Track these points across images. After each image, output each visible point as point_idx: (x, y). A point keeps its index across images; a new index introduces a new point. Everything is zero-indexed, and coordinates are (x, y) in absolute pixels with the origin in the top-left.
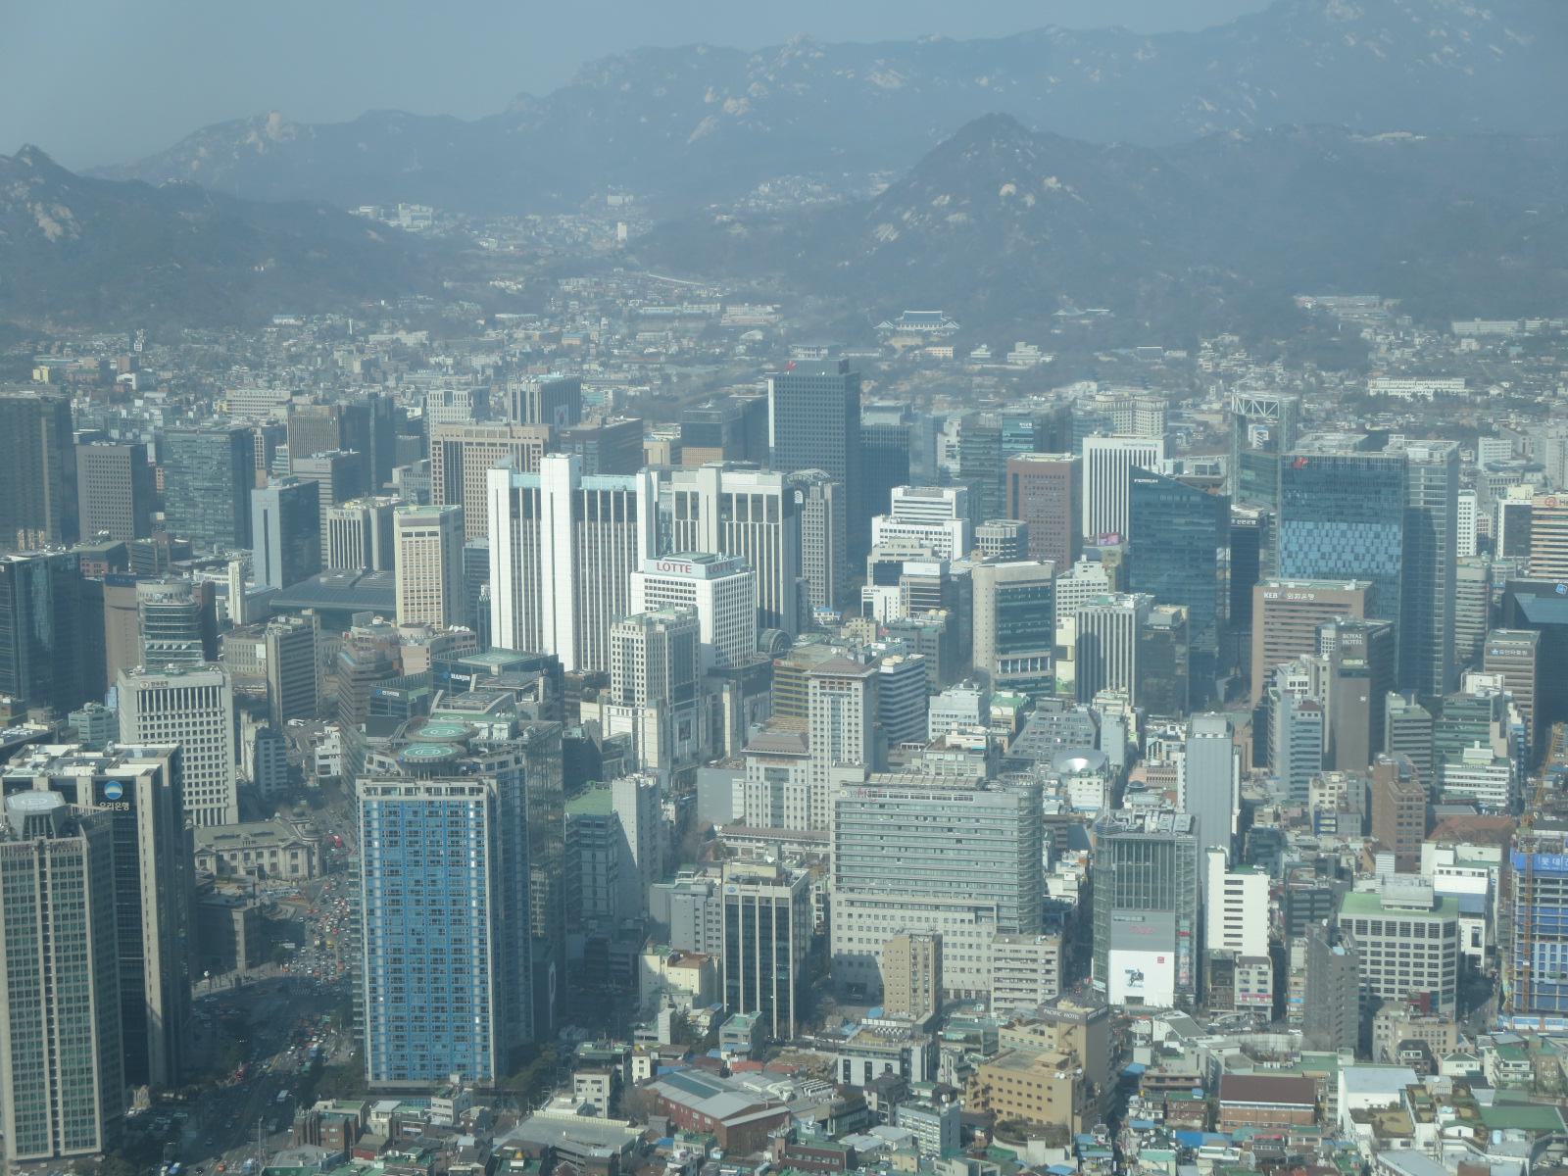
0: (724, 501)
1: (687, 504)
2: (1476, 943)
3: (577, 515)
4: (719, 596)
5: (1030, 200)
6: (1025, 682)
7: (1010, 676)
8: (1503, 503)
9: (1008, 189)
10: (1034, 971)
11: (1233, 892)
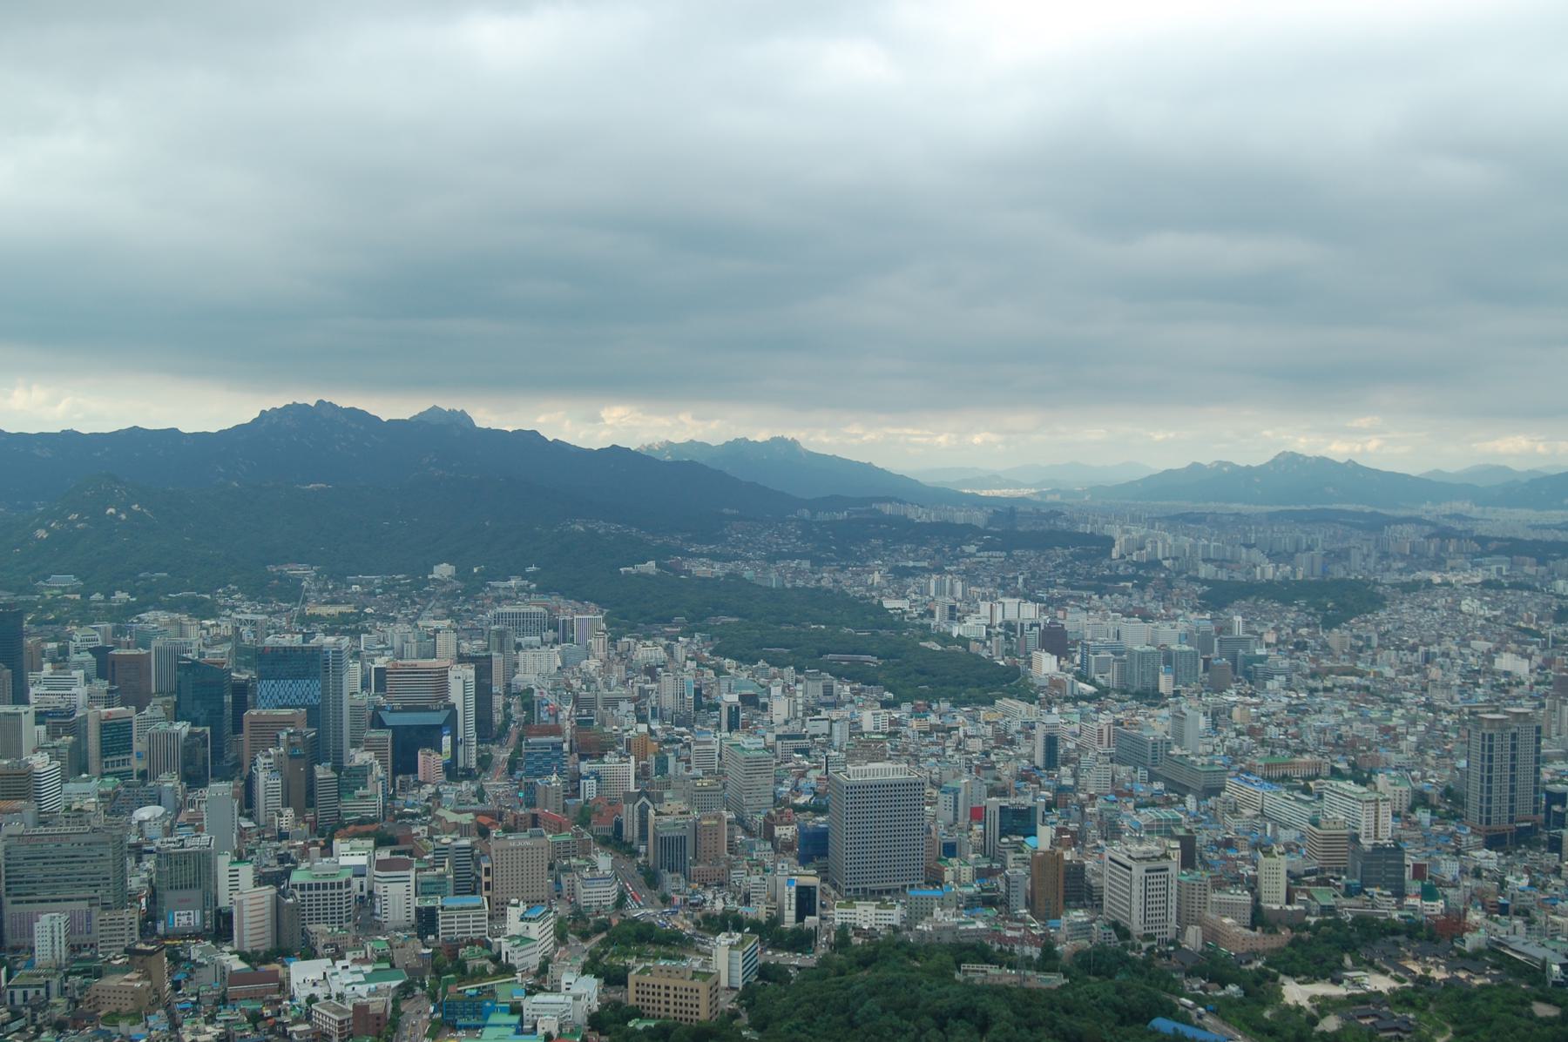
2: (362, 889)
5: (123, 516)
6: (114, 773)
7: (111, 770)
8: (374, 666)
9: (111, 510)
10: (123, 929)
11: (234, 875)
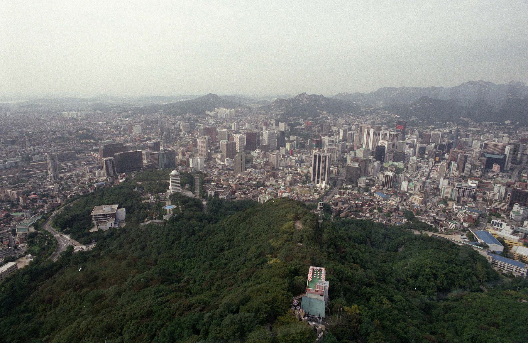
0: (390, 134)
1: (386, 135)
3: (374, 135)
4: (388, 144)
5: (428, 105)
7: (420, 156)
9: (426, 104)
